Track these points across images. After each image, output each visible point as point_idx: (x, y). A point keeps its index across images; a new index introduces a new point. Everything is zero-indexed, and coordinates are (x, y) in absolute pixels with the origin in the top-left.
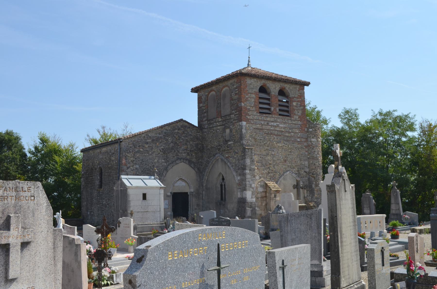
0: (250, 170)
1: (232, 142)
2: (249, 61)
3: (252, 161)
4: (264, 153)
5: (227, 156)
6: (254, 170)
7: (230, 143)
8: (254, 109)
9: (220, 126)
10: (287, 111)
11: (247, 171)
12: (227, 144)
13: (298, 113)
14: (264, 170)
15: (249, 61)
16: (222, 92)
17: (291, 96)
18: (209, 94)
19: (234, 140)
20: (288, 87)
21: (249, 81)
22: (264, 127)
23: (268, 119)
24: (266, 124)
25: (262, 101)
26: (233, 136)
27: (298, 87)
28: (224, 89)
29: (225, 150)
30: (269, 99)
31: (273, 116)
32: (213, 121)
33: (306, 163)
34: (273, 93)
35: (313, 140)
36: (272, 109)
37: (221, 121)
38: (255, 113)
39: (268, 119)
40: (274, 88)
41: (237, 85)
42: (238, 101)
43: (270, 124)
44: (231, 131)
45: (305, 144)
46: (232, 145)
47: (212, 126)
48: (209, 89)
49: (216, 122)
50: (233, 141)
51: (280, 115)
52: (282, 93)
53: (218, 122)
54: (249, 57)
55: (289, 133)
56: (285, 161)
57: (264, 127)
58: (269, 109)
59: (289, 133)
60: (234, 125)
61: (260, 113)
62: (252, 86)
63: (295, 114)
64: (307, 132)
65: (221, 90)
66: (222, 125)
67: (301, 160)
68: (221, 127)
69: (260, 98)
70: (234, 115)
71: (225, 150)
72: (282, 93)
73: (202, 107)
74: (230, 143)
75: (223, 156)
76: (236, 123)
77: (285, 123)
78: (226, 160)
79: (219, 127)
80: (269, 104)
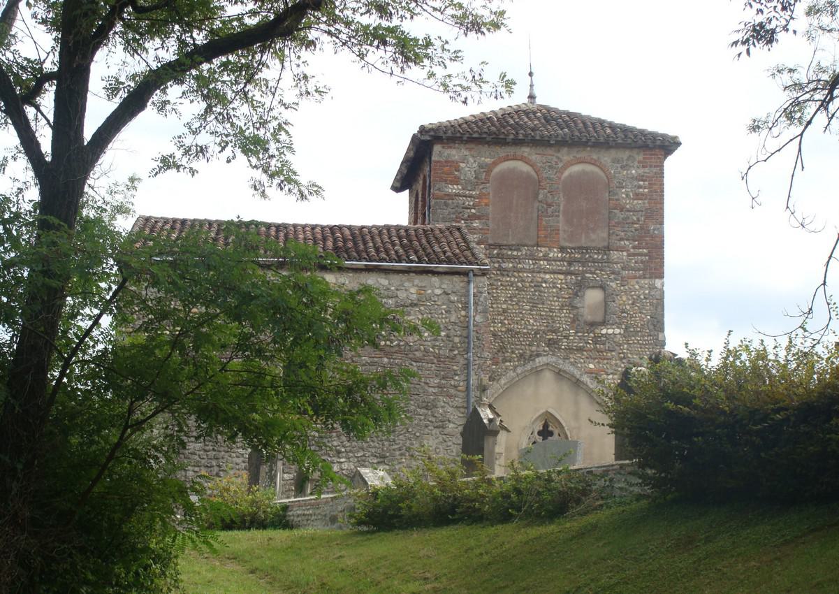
1: (617, 331)
2: (531, 86)
5: (591, 366)
7: (610, 331)
9: (554, 272)
12: (593, 332)
15: (531, 86)
16: (566, 173)
18: (495, 164)
19: (626, 330)
26: (622, 313)
28: (577, 168)
29: (580, 350)
32: (518, 250)
37: (562, 260)
41: (647, 170)
42: (647, 218)
44: (609, 297)
46: (619, 339)
47: (511, 265)
48: (502, 151)
49: (536, 259)
50: (623, 327)
53: (545, 258)
54: (531, 74)
60: (624, 281)
65: (565, 167)
66: (571, 273)
68: (562, 277)
70: (625, 253)
71: (580, 350)
73: (458, 195)
74: (610, 331)
75: (572, 364)
76: (635, 277)
78: (588, 380)
79: (548, 276)
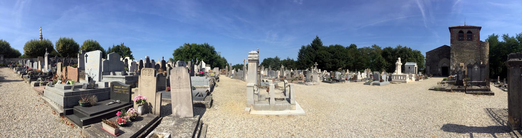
0: (452, 59)
3: (453, 57)
4: (460, 54)
6: (454, 59)
8: (456, 39)
10: (472, 39)
11: (451, 60)
13: (475, 40)
14: (459, 59)
17: (473, 33)
20: (471, 30)
21: (454, 30)
22: (460, 45)
23: (462, 42)
24: (461, 44)
25: (468, 36)
27: (476, 29)
30: (463, 35)
31: (465, 41)
33: (479, 56)
34: (464, 33)
35: (483, 48)
36: (464, 38)
38: (456, 40)
39: (462, 42)
40: (465, 31)
43: (463, 44)
45: (479, 50)
51: (468, 40)
52: (469, 32)
55: (472, 46)
56: (469, 56)
57: (460, 45)
58: (463, 39)
59: (472, 46)
61: (459, 40)
62: (455, 32)
63: (474, 39)
64: (480, 45)
67: (476, 55)
69: (459, 35)
72: (469, 32)
77: (469, 43)
80: (463, 37)
